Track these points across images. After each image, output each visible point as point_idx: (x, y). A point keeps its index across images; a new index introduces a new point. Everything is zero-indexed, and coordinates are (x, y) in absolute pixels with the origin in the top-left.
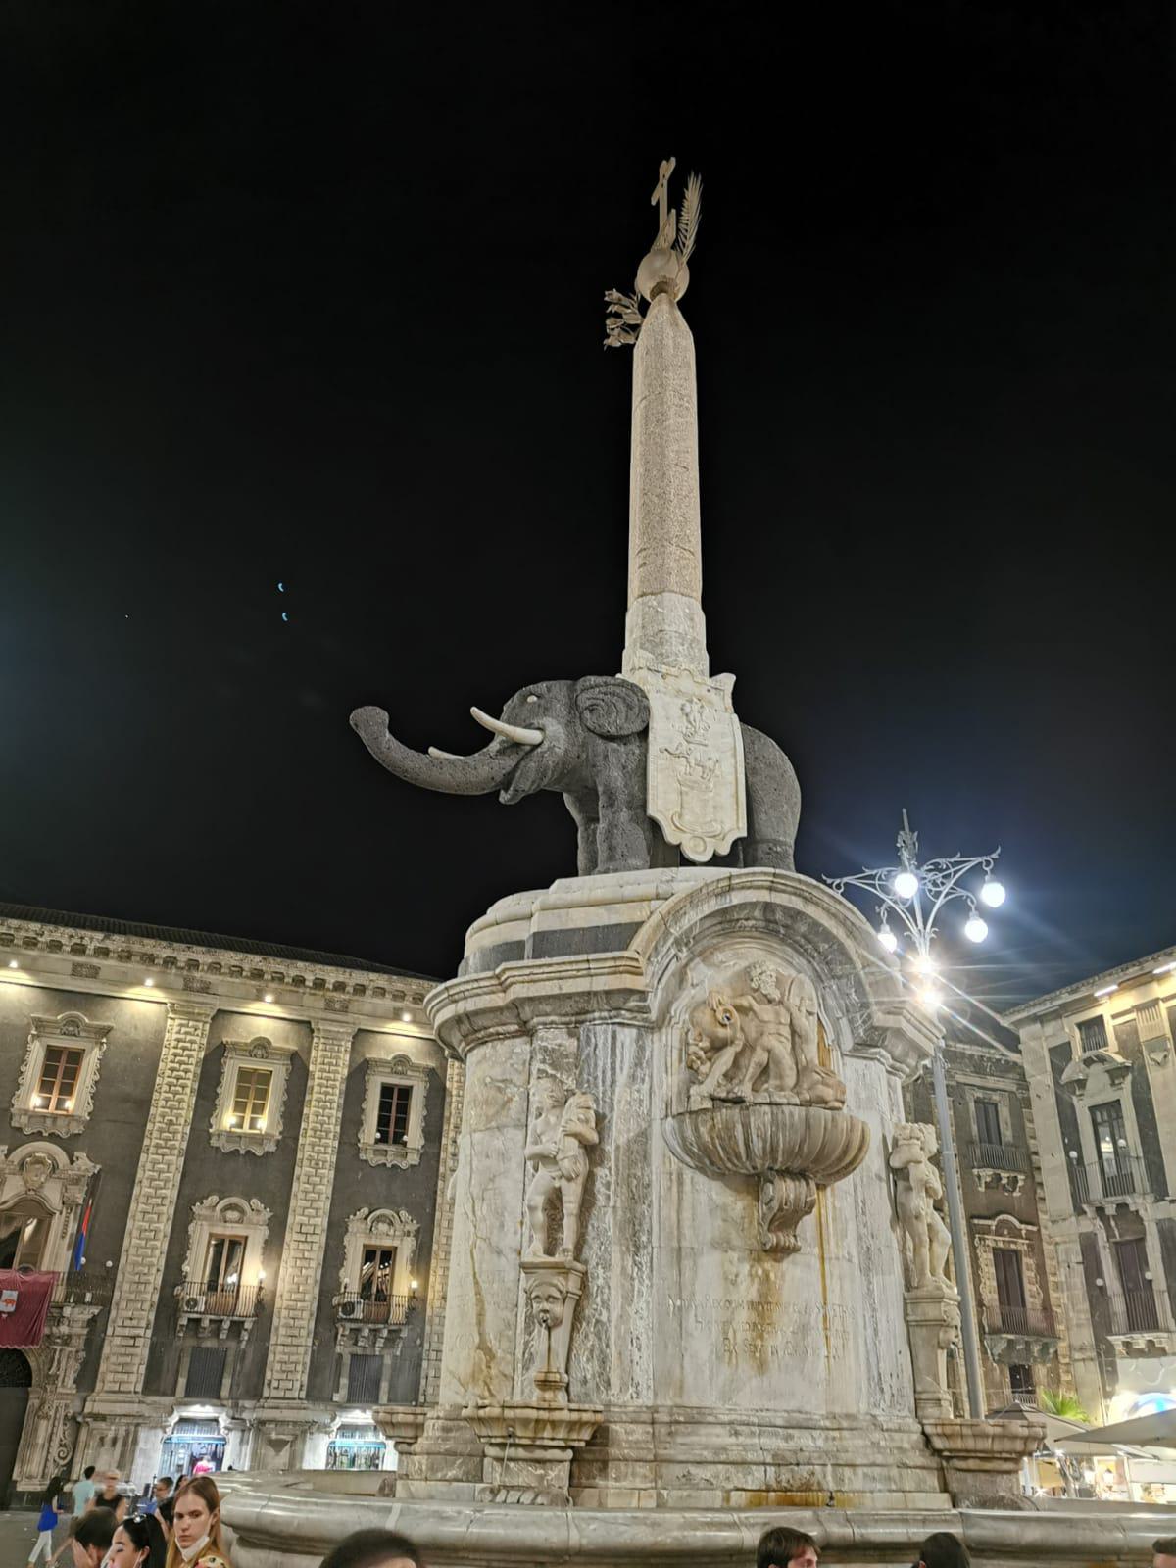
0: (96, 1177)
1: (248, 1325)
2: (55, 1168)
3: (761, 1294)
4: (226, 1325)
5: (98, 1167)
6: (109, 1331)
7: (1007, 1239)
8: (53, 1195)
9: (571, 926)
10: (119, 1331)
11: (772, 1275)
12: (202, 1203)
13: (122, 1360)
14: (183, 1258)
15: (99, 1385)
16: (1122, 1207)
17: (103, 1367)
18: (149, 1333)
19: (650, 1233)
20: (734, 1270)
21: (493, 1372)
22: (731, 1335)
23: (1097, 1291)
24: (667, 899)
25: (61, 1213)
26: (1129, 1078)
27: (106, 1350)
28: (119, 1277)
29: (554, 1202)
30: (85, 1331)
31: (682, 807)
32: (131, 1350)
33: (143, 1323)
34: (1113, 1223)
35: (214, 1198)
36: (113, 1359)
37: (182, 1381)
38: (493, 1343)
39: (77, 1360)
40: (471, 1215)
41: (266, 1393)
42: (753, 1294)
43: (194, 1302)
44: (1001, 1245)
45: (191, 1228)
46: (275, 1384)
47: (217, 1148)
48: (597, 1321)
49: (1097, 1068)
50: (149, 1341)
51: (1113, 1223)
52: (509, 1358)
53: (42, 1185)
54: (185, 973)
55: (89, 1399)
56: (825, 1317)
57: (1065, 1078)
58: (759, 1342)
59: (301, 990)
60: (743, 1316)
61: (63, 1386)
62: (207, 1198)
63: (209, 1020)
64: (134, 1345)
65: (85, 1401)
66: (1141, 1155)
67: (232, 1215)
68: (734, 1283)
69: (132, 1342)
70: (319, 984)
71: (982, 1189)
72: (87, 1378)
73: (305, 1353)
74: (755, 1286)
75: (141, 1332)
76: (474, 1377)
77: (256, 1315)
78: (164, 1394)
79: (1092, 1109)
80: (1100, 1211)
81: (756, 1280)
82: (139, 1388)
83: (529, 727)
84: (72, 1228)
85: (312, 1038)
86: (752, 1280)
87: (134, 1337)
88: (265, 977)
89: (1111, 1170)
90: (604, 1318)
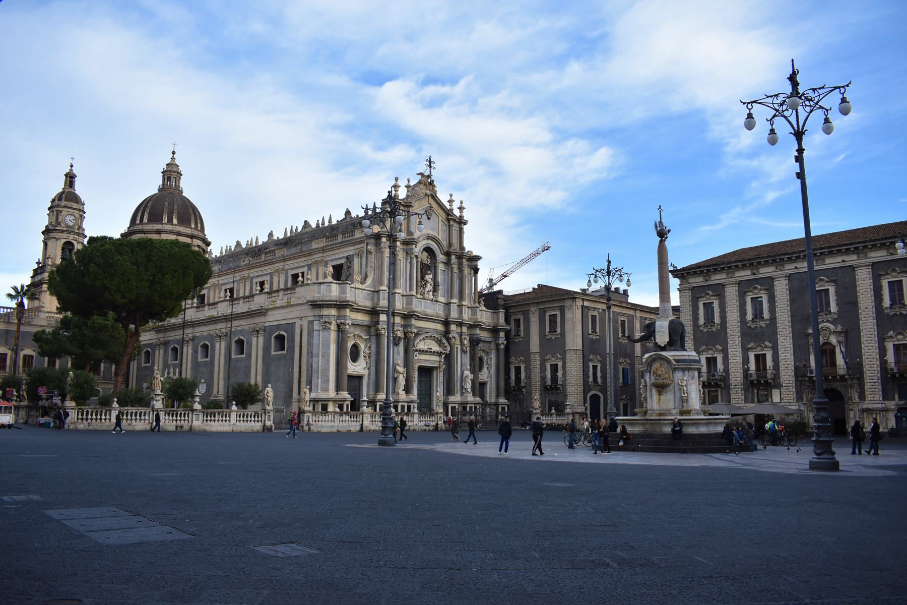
2: (831, 331)
6: (865, 381)
13: (872, 390)
14: (885, 355)
15: (867, 399)
17: (866, 393)
18: (880, 381)
27: (866, 387)
28: (864, 364)
32: (874, 387)
33: (876, 378)
37: (896, 396)
39: (857, 391)
45: (885, 343)
50: (880, 383)
53: (829, 338)
54: (856, 252)
60: (658, 401)
62: (889, 332)
67: (900, 337)
72: (862, 397)
78: (891, 400)
82: (881, 399)
87: (875, 382)
88: (887, 244)
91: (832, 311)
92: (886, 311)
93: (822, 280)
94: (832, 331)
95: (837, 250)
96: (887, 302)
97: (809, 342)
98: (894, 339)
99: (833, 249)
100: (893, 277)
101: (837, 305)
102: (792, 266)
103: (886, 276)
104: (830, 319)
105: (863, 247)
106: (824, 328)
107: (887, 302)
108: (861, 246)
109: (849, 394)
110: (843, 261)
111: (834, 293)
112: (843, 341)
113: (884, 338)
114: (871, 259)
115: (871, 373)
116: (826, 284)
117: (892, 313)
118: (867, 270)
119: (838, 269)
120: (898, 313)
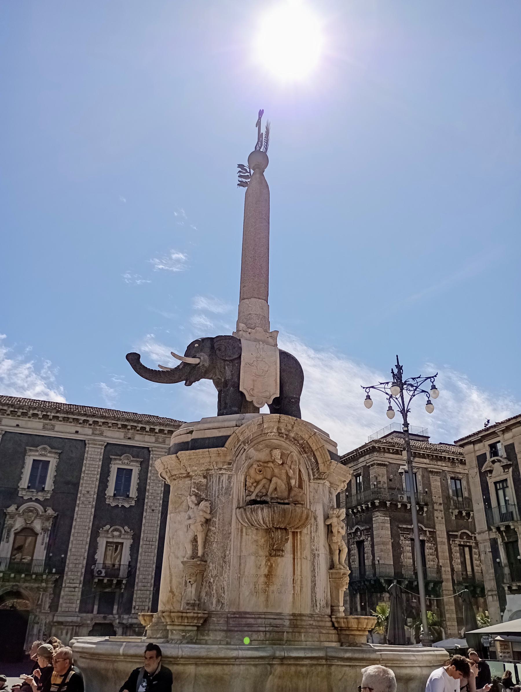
0: (56, 518)
1: (124, 582)
2: (38, 514)
3: (269, 572)
4: (115, 582)
5: (57, 513)
6: (63, 585)
7: (465, 540)
8: (37, 526)
9: (206, 437)
10: (67, 585)
11: (274, 565)
12: (103, 529)
13: (69, 597)
14: (95, 553)
15: (59, 609)
16: (508, 527)
18: (81, 586)
19: (230, 550)
20: (259, 564)
21: (174, 600)
22: (257, 586)
23: (497, 565)
24: (239, 426)
25: (41, 534)
26: (511, 469)
28: (67, 561)
29: (195, 540)
30: (53, 586)
31: (254, 386)
32: (73, 593)
33: (78, 582)
34: (504, 534)
35: (108, 527)
36: (65, 597)
37: (96, 607)
38: (175, 590)
40: (169, 544)
41: (133, 612)
42: (266, 572)
43: (100, 572)
44: (462, 543)
45: (98, 539)
46: (137, 607)
47: (109, 504)
48: (210, 582)
49: (497, 464)
50: (81, 590)
51: (504, 534)
52: (180, 595)
53: (32, 522)
54: (92, 427)
55: (56, 615)
56: (294, 580)
57: (483, 470)
58: (267, 589)
59: (144, 433)
60: (262, 579)
61: (44, 609)
62: (105, 527)
63: (103, 447)
64: (75, 591)
65: (54, 616)
66: (516, 503)
67: (116, 533)
68: (259, 568)
69: (73, 590)
70: (152, 430)
71: (454, 518)
72: (54, 607)
73: (150, 594)
74: (267, 569)
75: (77, 585)
76: (168, 602)
77: (127, 577)
78: (88, 612)
79: (495, 483)
80: (498, 529)
81: (268, 567)
82: (77, 610)
83: (194, 357)
84: (47, 540)
85: (150, 455)
86: (266, 567)
87: (75, 588)
89: (504, 511)
90: (212, 581)
91: (46, 489)
92: (107, 500)
93: (44, 449)
94: (41, 513)
95: (74, 419)
96: (111, 491)
97: (4, 524)
98: (109, 535)
99: (70, 416)
100: (123, 464)
101: (54, 483)
102: (14, 423)
103: (118, 462)
104: (41, 499)
105: (104, 423)
106: (32, 509)
107: (111, 491)
108: (101, 422)
109: (40, 600)
110: (77, 432)
111: (54, 467)
112: (50, 528)
113: (98, 531)
114: (107, 439)
115: (74, 575)
116: (49, 455)
117: (113, 504)
118: (99, 450)
119: (66, 440)
120: (120, 506)
